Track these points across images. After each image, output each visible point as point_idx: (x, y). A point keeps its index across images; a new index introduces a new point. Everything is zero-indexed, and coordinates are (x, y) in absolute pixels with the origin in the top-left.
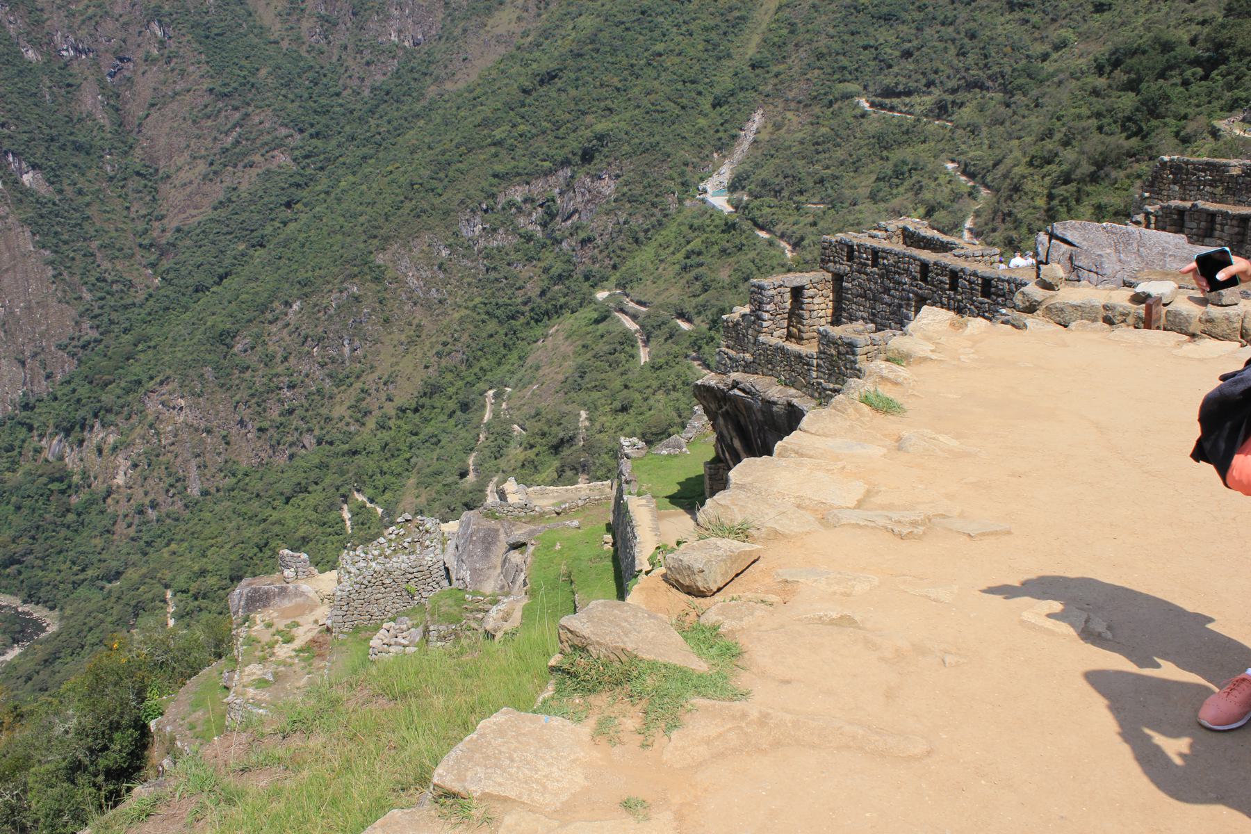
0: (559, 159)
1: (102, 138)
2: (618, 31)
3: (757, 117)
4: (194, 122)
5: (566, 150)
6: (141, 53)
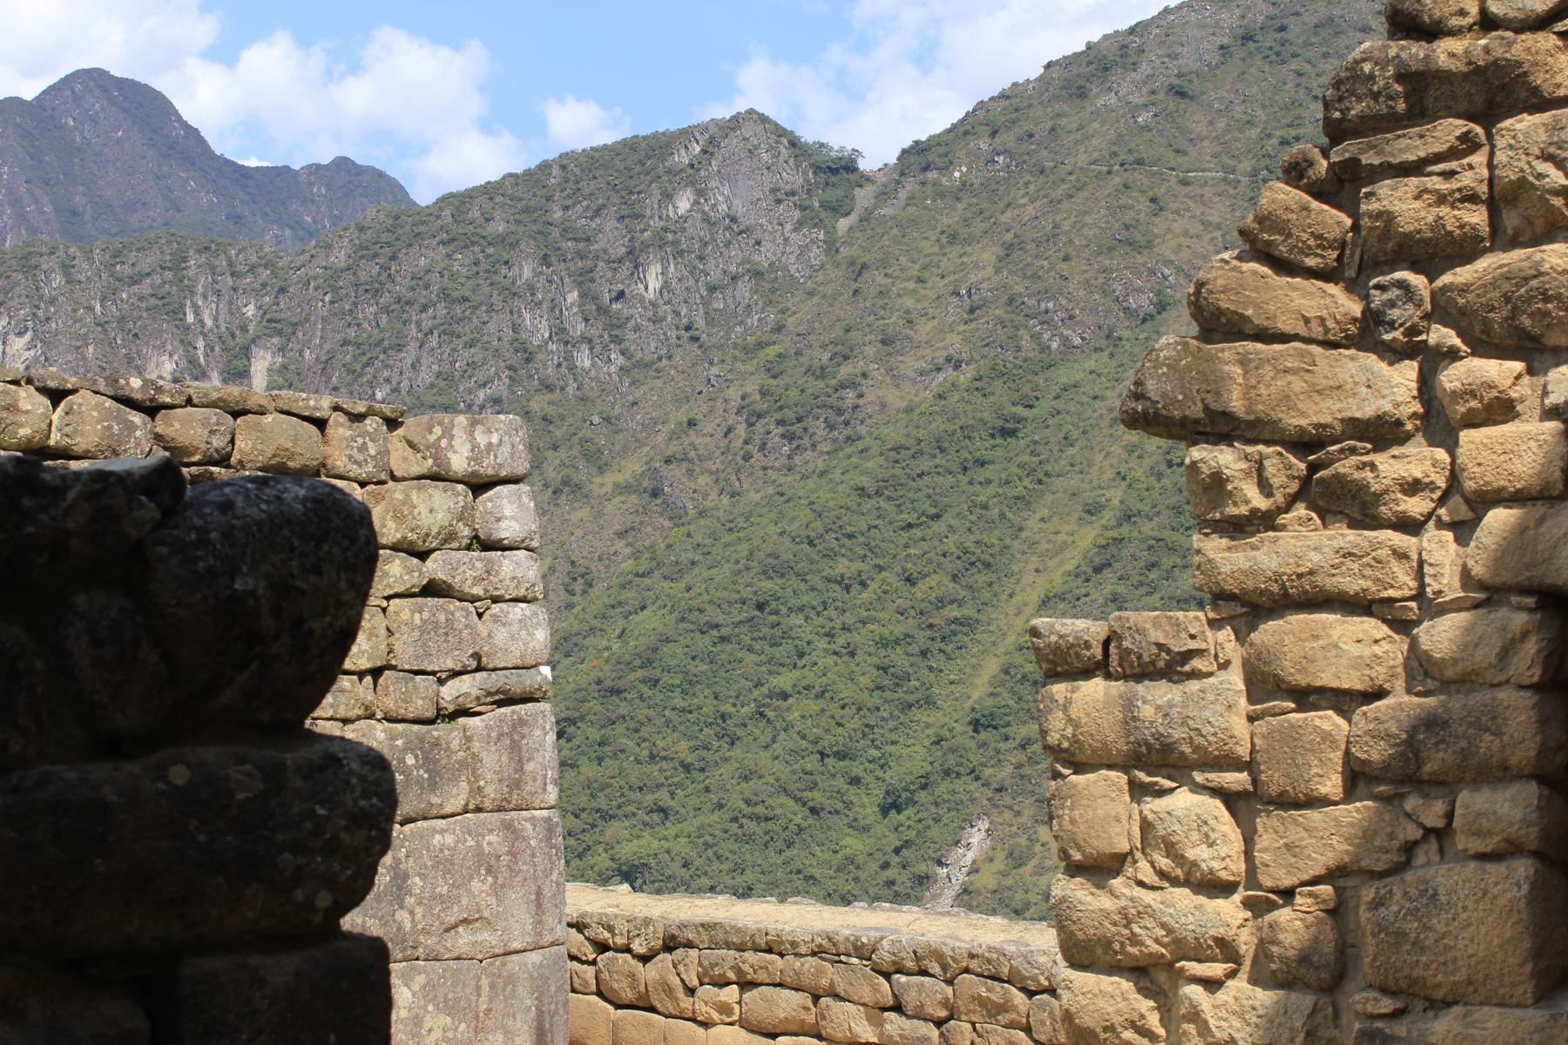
3: (976, 837)
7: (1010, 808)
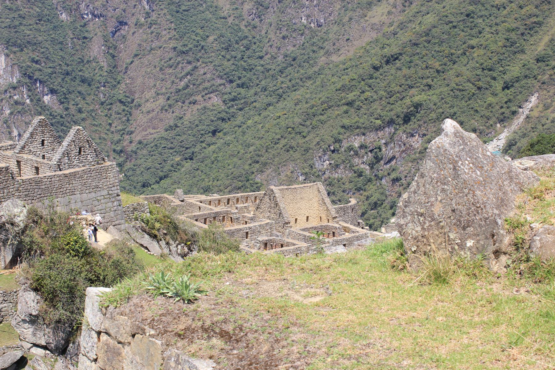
0: (387, 119)
1: (101, 75)
2: (447, 27)
3: (533, 99)
4: (161, 69)
5: (392, 113)
6: (133, 20)
7: (546, 89)
